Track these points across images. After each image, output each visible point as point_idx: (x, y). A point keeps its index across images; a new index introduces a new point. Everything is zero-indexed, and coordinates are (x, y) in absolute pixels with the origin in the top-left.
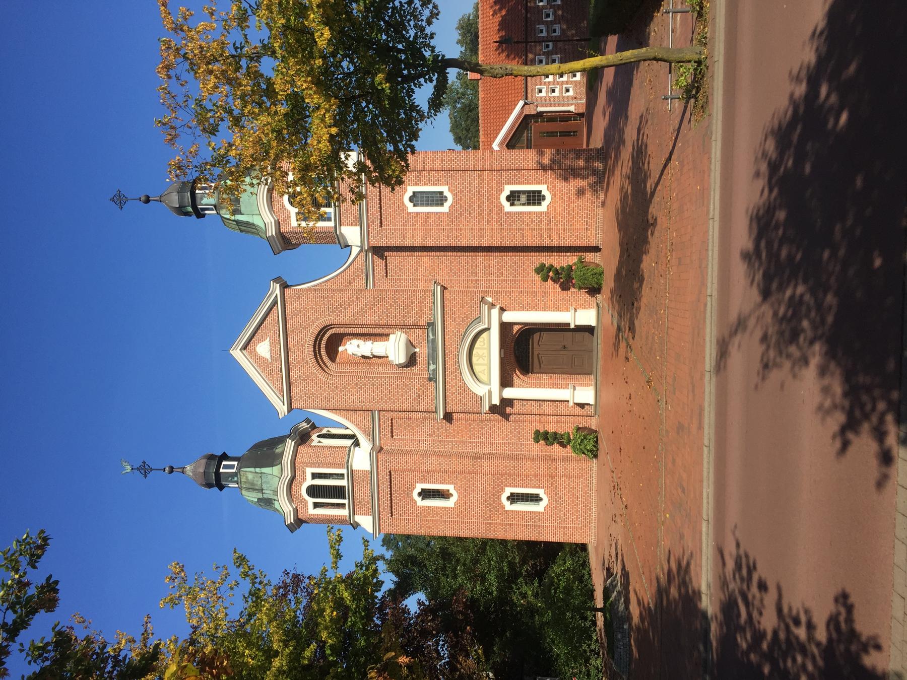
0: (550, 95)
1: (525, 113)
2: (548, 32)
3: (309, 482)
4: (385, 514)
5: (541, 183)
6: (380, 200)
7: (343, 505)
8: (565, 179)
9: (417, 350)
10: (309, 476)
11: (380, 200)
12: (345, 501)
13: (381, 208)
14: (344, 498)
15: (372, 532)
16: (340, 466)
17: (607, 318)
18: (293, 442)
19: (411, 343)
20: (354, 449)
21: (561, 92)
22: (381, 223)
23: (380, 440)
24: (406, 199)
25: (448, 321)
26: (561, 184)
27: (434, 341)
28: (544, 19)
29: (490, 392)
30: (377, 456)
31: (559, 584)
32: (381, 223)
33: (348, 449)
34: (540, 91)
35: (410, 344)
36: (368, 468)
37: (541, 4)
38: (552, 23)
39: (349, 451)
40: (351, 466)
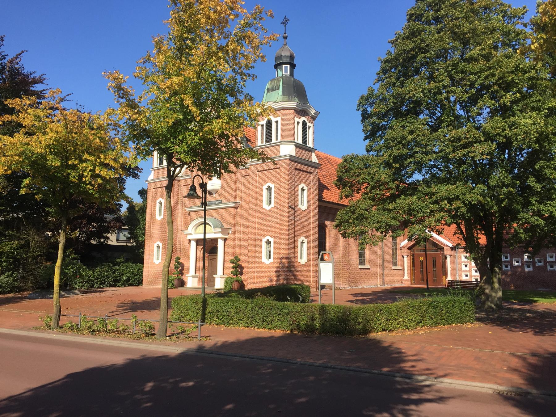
0: (463, 264)
1: (445, 248)
2: (505, 262)
3: (273, 119)
4: (154, 185)
5: (274, 259)
6: (268, 170)
7: (262, 142)
8: (276, 272)
9: (214, 195)
10: (276, 119)
11: (268, 170)
12: (264, 143)
13: (265, 170)
14: (266, 142)
15: (149, 179)
16: (282, 138)
17: (189, 293)
18: (295, 107)
19: (217, 192)
20: (292, 144)
21: (464, 271)
22: (259, 171)
23: (183, 179)
24: (269, 184)
25: (223, 211)
26: (274, 269)
27: (215, 204)
28: (514, 259)
29: (190, 234)
30: (285, 159)
31: (67, 269)
32: (259, 171)
33: (293, 140)
34: (551, 257)
35: (216, 191)
36: (281, 154)
37: (526, 257)
38: (512, 264)
39: (291, 142)
40: (282, 144)
